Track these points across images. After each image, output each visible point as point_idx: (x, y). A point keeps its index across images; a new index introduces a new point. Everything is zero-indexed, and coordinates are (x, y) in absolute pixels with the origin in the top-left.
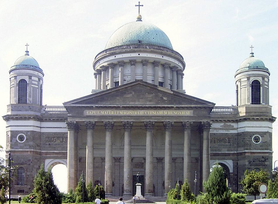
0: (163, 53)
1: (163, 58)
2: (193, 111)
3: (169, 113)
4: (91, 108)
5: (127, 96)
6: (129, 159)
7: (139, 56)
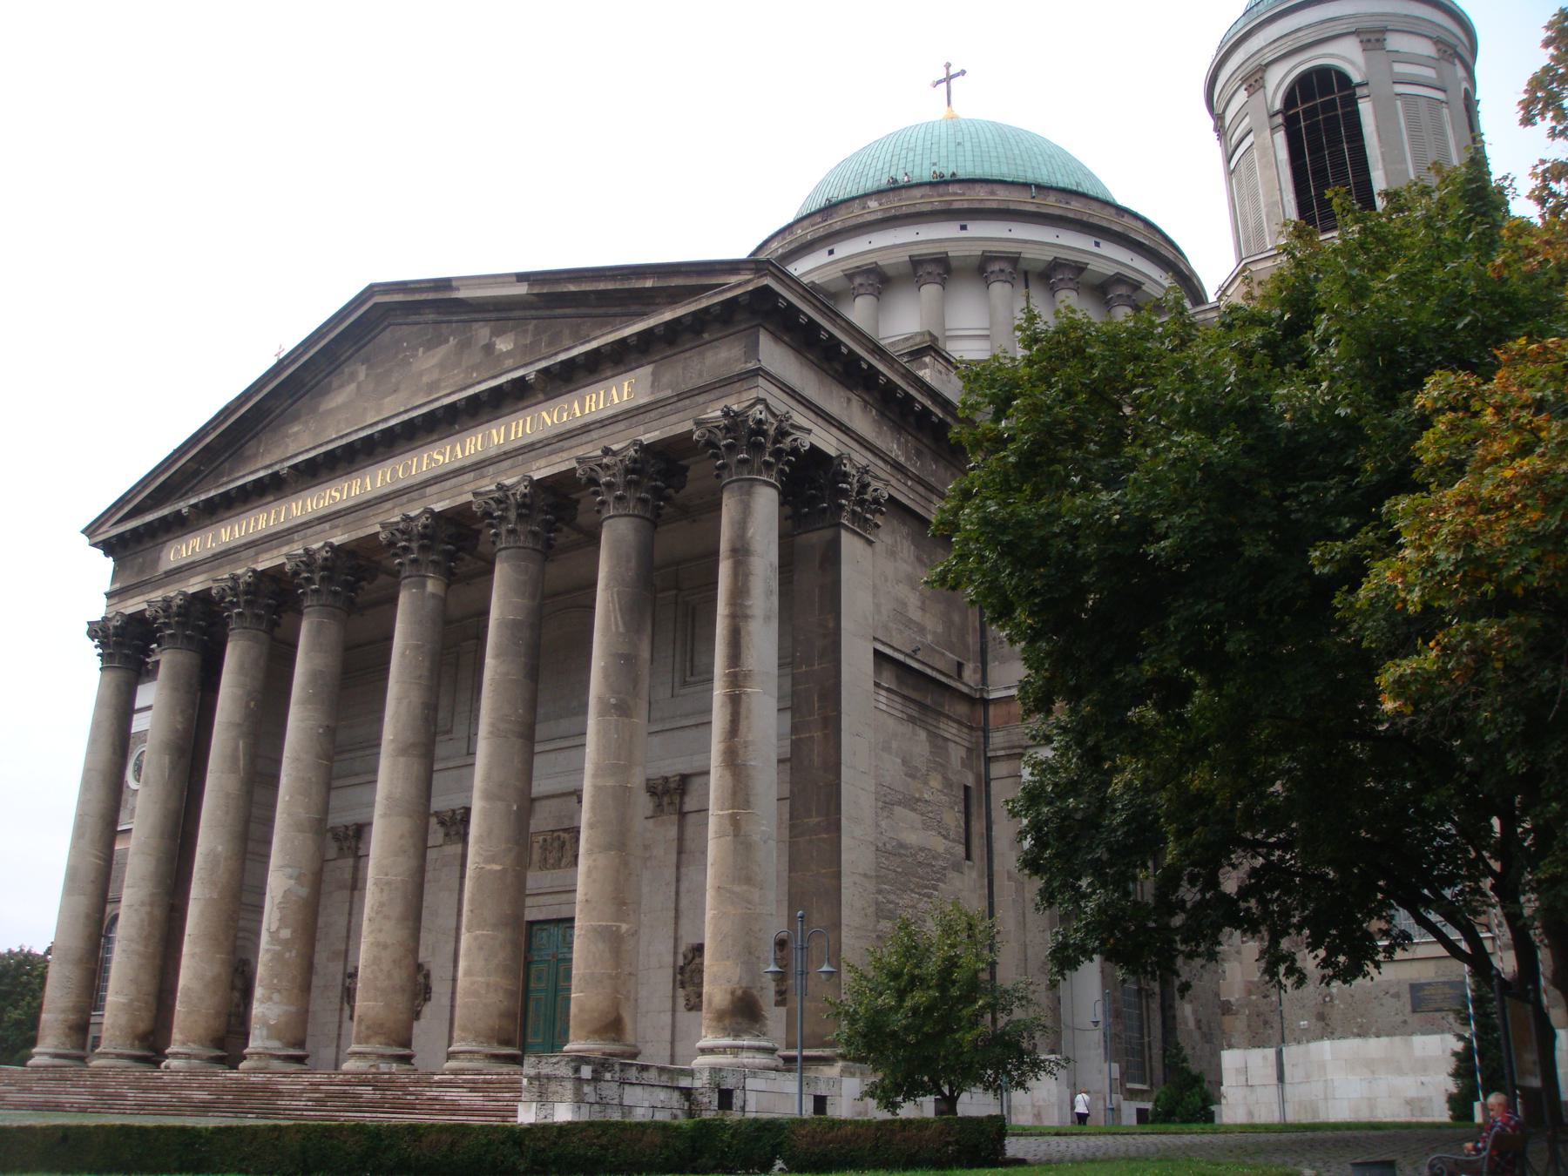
0: (956, 206)
1: (963, 234)
2: (648, 369)
3: (516, 432)
4: (178, 526)
5: (332, 404)
6: (291, 797)
7: (832, 258)
